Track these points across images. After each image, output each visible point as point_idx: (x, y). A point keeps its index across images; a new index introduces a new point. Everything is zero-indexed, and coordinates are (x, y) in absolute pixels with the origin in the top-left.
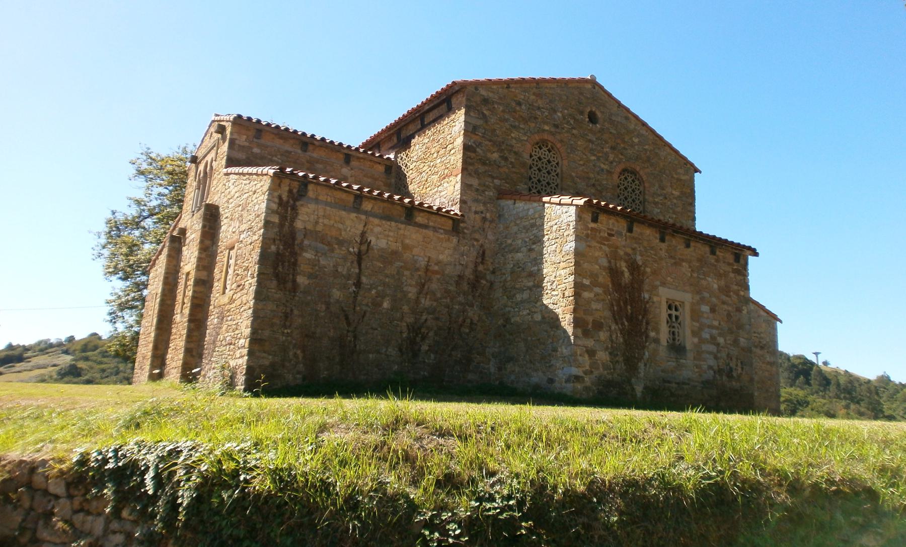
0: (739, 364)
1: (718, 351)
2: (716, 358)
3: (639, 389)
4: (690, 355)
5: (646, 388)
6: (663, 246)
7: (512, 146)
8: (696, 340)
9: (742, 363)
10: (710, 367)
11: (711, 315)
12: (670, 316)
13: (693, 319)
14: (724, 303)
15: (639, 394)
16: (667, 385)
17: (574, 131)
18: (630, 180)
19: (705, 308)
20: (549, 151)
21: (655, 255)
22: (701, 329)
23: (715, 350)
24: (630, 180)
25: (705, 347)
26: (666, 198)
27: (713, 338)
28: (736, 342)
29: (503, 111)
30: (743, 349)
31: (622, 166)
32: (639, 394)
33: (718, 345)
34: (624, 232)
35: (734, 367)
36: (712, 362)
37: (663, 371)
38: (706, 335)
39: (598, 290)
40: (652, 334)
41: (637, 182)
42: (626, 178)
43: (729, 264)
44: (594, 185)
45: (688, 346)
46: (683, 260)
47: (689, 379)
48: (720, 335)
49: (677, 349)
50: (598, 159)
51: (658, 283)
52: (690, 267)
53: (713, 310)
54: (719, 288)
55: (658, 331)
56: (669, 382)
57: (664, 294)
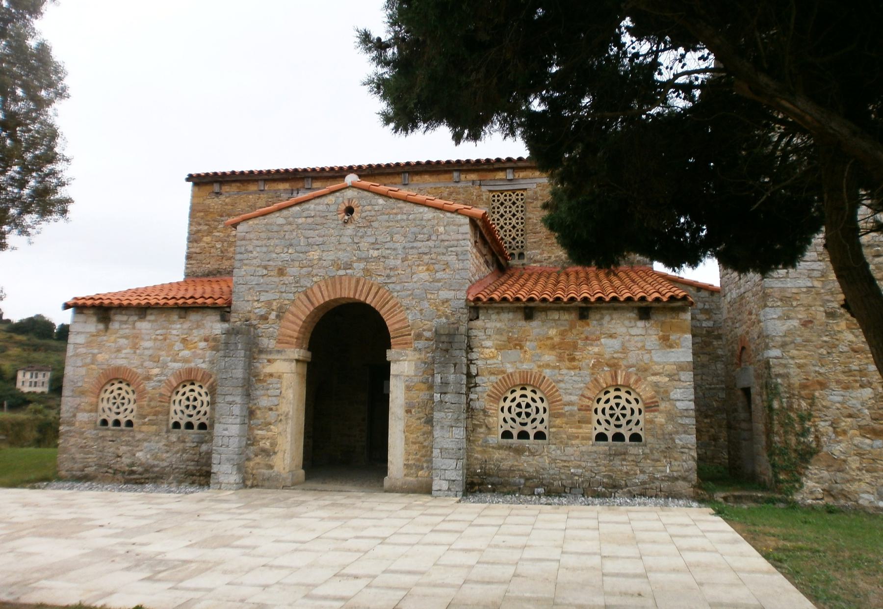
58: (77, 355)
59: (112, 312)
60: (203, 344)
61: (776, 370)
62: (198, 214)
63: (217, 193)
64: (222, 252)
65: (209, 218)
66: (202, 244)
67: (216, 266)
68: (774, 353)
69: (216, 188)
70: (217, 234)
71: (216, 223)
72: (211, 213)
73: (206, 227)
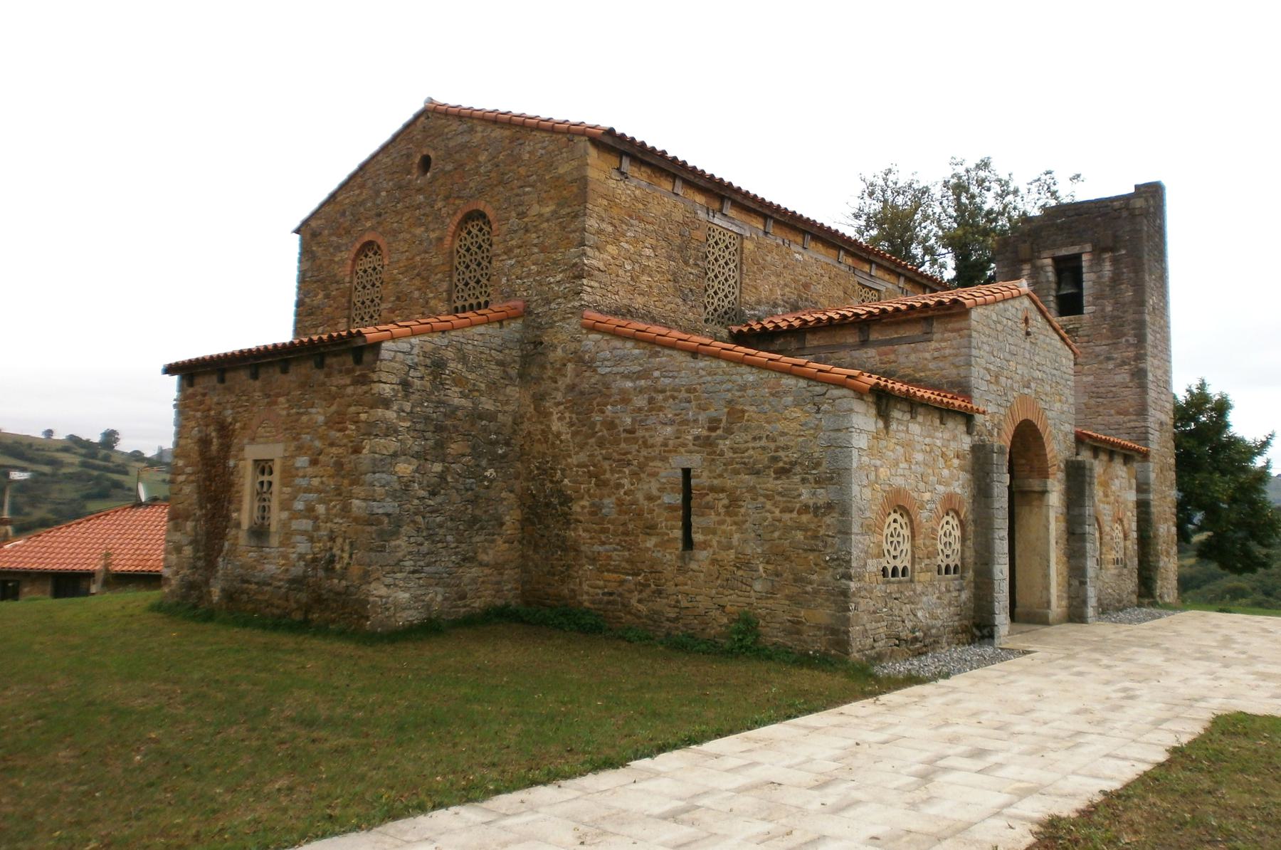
0: (347, 548)
1: (317, 528)
2: (311, 540)
3: (216, 593)
4: (274, 541)
5: (223, 590)
6: (258, 383)
7: (335, 275)
8: (285, 515)
9: (351, 544)
10: (301, 557)
11: (310, 470)
12: (262, 483)
13: (284, 485)
14: (332, 445)
15: (215, 598)
16: (245, 586)
17: (400, 206)
18: (475, 231)
19: (302, 461)
20: (375, 254)
21: (247, 401)
22: (294, 498)
23: (310, 528)
24: (475, 231)
25: (295, 525)
26: (527, 231)
27: (310, 511)
28: (346, 509)
29: (330, 235)
30: (356, 520)
31: (459, 216)
32: (215, 598)
33: (316, 518)
34: (218, 385)
35: (338, 553)
36: (303, 547)
37: (242, 567)
38: (299, 505)
39: (189, 470)
40: (235, 515)
41: (486, 229)
42: (469, 233)
43: (349, 372)
44: (418, 275)
45: (273, 528)
46: (278, 395)
47: (271, 577)
48: (321, 501)
49: (260, 533)
50: (427, 230)
51: (246, 441)
52: (288, 401)
53: (314, 462)
54: (329, 423)
55: (238, 510)
56: (248, 582)
57: (253, 452)
58: (860, 468)
59: (892, 403)
60: (956, 462)
61: (1153, 510)
62: (600, 200)
63: (622, 173)
64: (632, 279)
65: (615, 212)
66: (605, 256)
67: (626, 302)
68: (1151, 497)
69: (626, 165)
70: (626, 246)
71: (625, 227)
72: (616, 205)
73: (610, 229)
